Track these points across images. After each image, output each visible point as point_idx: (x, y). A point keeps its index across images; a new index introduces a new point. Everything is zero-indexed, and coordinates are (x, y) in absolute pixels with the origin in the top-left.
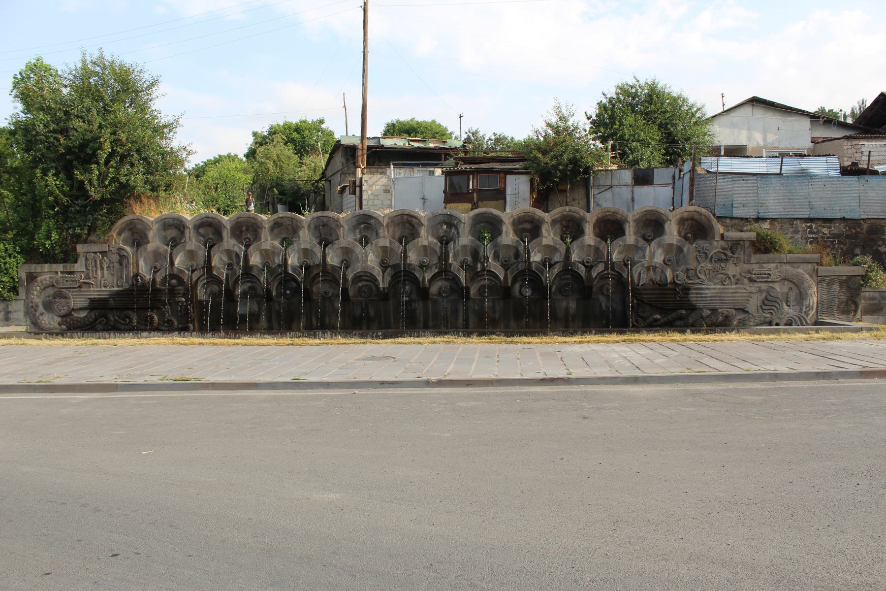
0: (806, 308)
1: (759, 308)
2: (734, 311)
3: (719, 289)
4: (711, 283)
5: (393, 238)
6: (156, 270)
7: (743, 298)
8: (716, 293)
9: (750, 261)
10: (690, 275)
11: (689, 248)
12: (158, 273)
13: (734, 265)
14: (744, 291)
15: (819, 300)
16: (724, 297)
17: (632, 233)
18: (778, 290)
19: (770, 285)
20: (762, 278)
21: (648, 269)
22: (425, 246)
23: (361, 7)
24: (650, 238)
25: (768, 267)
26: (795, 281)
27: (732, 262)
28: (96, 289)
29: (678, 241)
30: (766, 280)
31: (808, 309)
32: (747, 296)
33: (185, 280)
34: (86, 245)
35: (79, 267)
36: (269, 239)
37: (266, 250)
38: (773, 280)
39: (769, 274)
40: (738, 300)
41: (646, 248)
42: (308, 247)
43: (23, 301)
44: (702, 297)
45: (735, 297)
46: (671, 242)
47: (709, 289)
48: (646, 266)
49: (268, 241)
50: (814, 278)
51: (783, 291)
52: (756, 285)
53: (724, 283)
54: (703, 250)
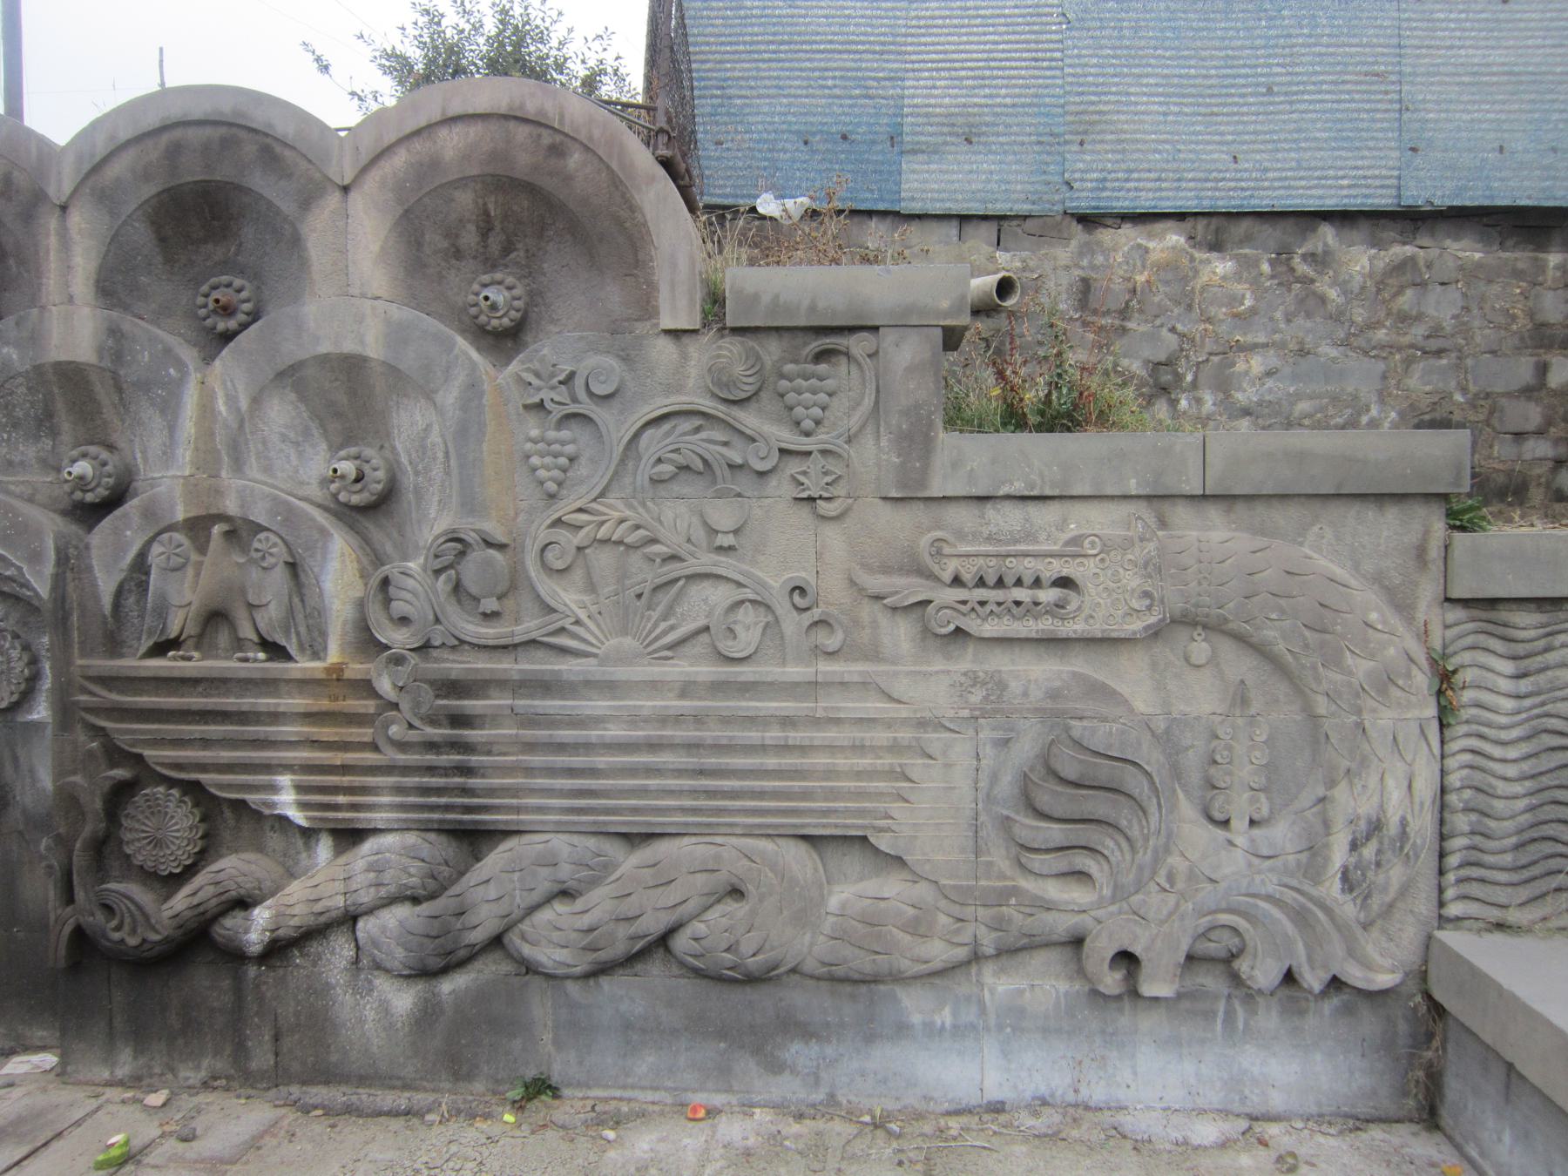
0: (1354, 846)
1: (989, 831)
2: (796, 857)
3: (686, 689)
4: (628, 642)
7: (865, 762)
8: (664, 720)
9: (923, 482)
10: (471, 584)
11: (473, 388)
13: (804, 511)
14: (873, 706)
15: (1454, 780)
16: (719, 748)
17: (82, 282)
18: (1142, 700)
19: (1079, 664)
21: (198, 527)
24: (232, 324)
25: (1062, 525)
26: (1270, 634)
27: (790, 491)
29: (397, 335)
30: (1045, 625)
31: (1369, 852)
32: (895, 748)
38: (1097, 629)
39: (1064, 582)
40: (830, 773)
41: (181, 382)
44: (561, 748)
45: (803, 749)
46: (349, 347)
47: (610, 687)
48: (180, 514)
50: (1421, 616)
51: (1179, 708)
52: (966, 661)
53: (727, 647)
54: (575, 400)
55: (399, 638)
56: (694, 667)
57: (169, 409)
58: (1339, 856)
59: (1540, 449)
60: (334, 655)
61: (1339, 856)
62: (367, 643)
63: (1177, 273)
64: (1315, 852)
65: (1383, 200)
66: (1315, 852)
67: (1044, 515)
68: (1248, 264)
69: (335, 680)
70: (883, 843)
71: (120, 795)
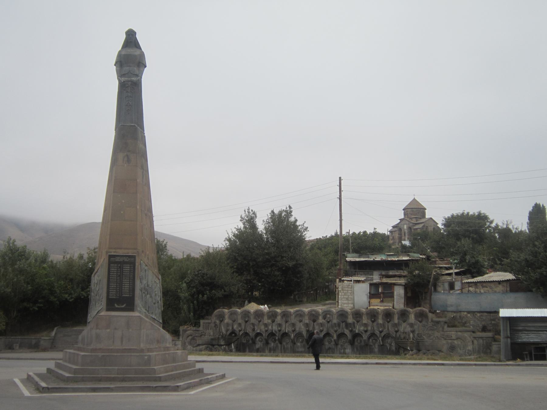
2: (437, 352)
3: (431, 342)
5: (310, 320)
6: (227, 331)
12: (228, 332)
14: (441, 343)
17: (397, 318)
20: (449, 338)
21: (403, 333)
22: (321, 323)
23: (338, 198)
28: (206, 337)
30: (450, 338)
33: (237, 334)
34: (203, 320)
35: (201, 328)
36: (267, 319)
37: (266, 324)
39: (451, 336)
42: (280, 323)
43: (181, 341)
47: (427, 342)
49: (266, 320)
55: (415, 339)
56: (431, 341)
57: (402, 326)
58: (467, 352)
59: (492, 328)
60: (411, 340)
61: (467, 352)
62: (413, 339)
63: (466, 315)
64: (465, 352)
65: (479, 311)
66: (465, 352)
67: (450, 332)
68: (471, 315)
69: (412, 341)
70: (442, 351)
71: (399, 348)
